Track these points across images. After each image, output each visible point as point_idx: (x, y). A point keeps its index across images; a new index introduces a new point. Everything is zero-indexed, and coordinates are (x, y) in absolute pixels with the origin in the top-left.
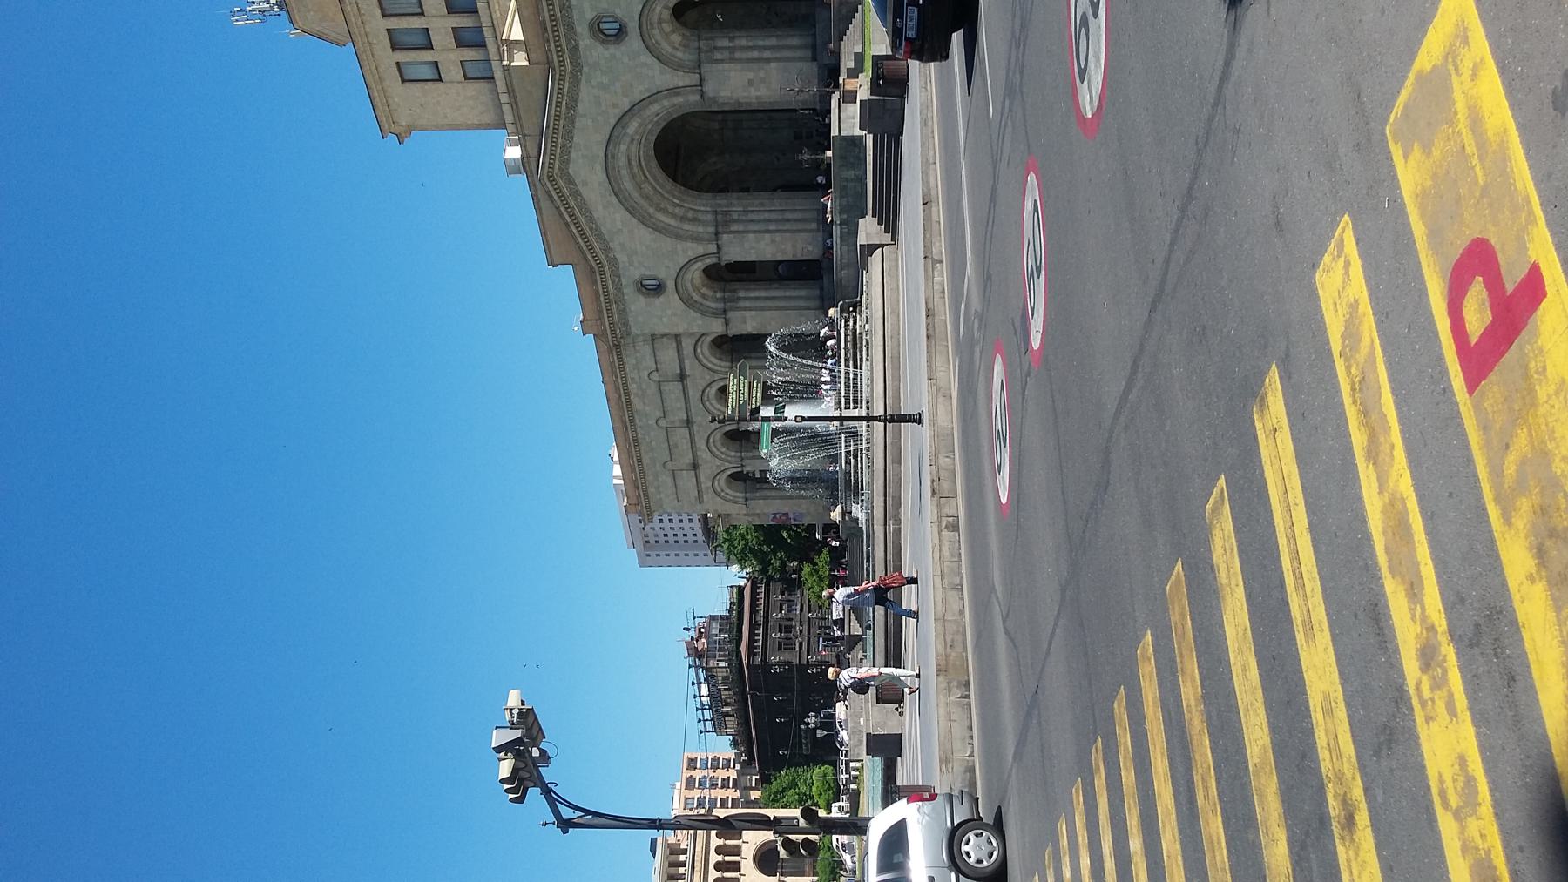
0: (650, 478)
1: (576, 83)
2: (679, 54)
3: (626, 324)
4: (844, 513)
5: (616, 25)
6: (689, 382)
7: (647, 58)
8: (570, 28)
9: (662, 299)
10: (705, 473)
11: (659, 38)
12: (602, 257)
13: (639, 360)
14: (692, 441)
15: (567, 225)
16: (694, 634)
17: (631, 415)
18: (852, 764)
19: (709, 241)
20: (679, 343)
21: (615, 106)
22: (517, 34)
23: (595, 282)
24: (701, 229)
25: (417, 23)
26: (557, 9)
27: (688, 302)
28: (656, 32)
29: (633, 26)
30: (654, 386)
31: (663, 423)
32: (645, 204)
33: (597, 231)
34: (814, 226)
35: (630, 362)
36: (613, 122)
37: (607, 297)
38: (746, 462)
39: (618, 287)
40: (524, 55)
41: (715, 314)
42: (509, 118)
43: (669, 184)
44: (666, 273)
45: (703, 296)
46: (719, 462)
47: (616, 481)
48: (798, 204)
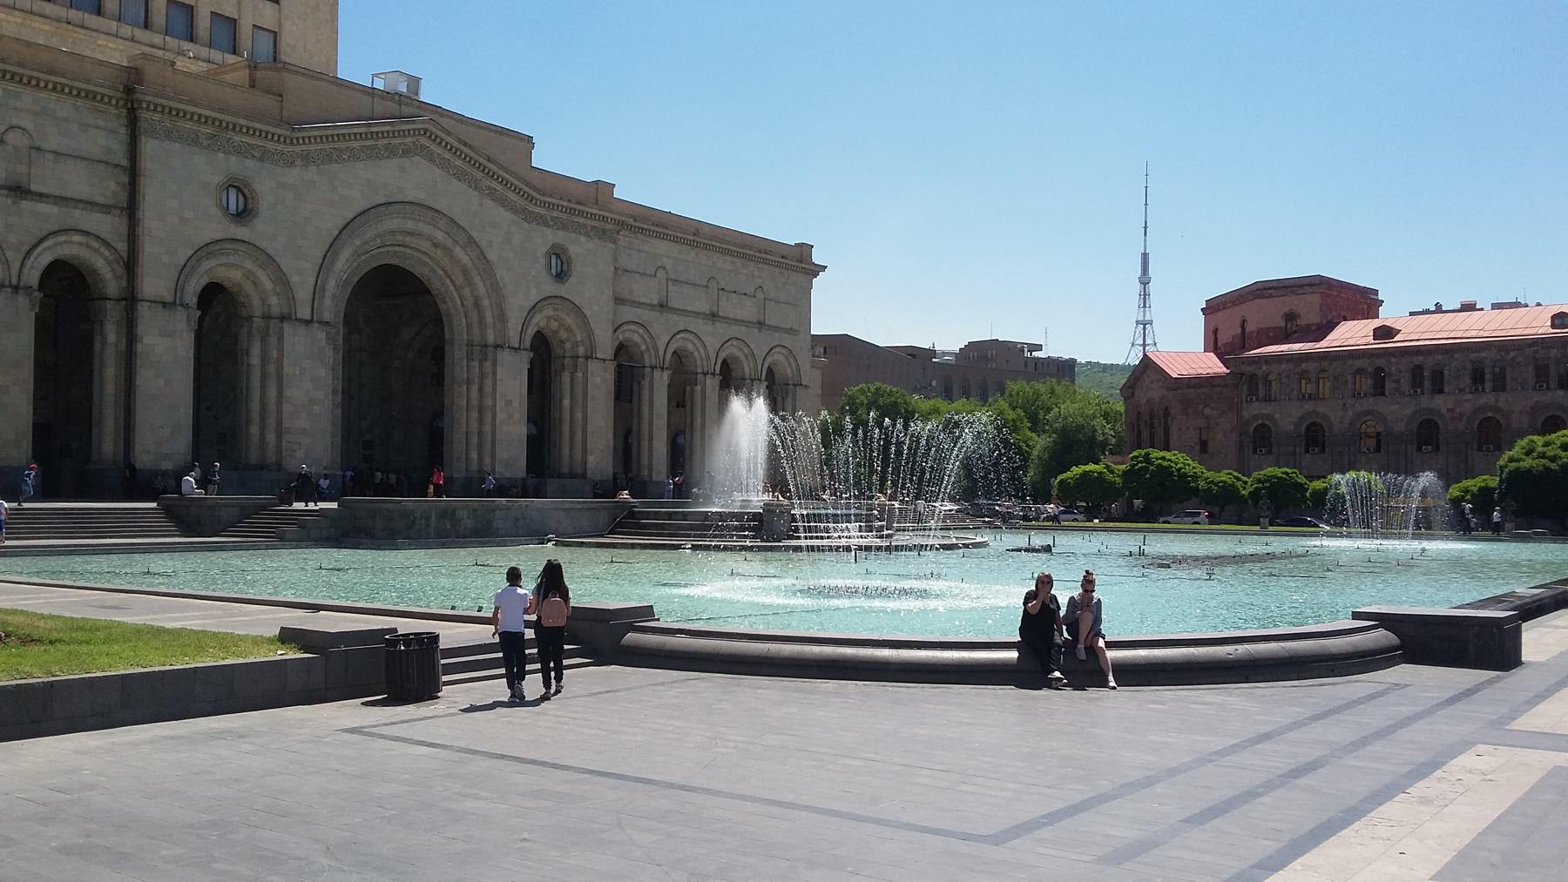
1: (514, 209)
3: (168, 135)
7: (534, 297)
8: (564, 226)
9: (215, 211)
12: (298, 149)
20: (105, 208)
26: (581, 220)
27: (206, 250)
28: (549, 311)
35: (64, 107)
36: (474, 234)
41: (178, 288)
44: (261, 230)
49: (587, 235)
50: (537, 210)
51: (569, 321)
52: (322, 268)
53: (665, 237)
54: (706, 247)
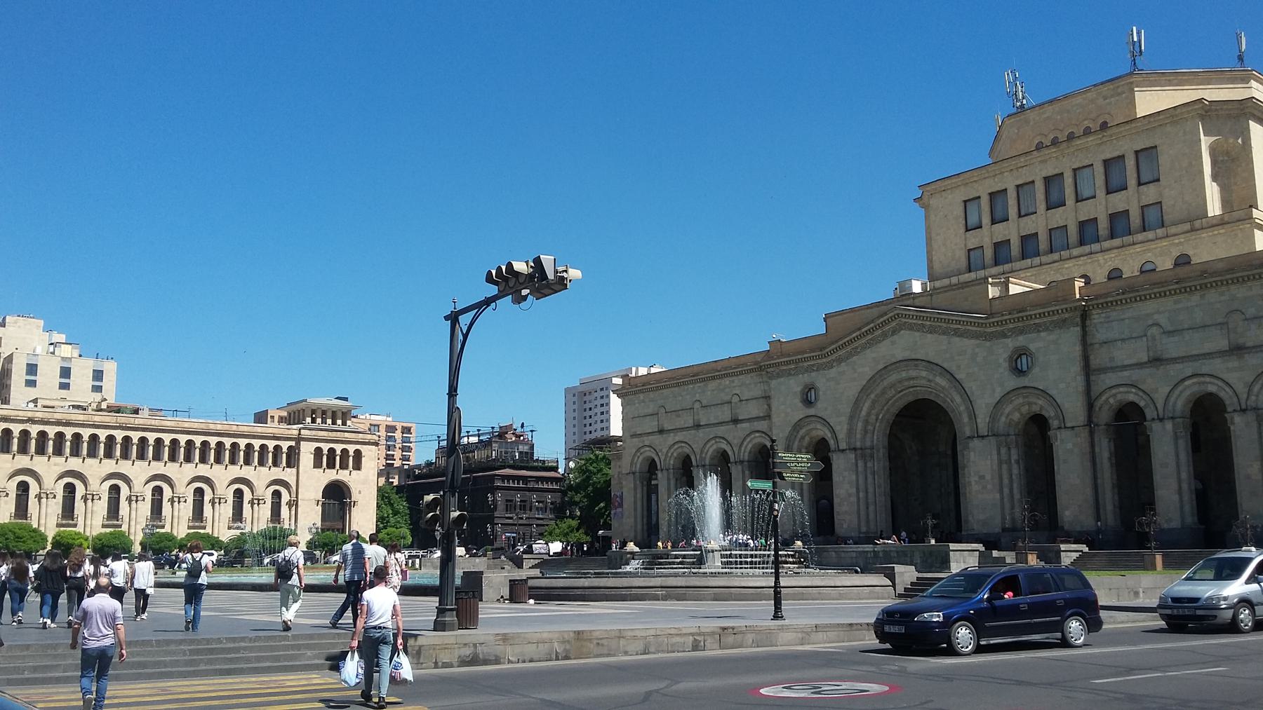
0: (652, 395)
1: (976, 336)
2: (1003, 419)
3: (779, 376)
4: (632, 553)
5: (1025, 368)
6: (731, 426)
8: (1021, 332)
9: (800, 404)
10: (656, 439)
11: (1016, 403)
12: (833, 357)
13: (749, 387)
14: (682, 429)
15: (860, 329)
16: (519, 430)
17: (703, 380)
19: (848, 443)
20: (763, 418)
21: (959, 367)
22: (1014, 289)
23: (812, 351)
24: (858, 436)
25: (1013, 212)
27: (797, 426)
28: (1021, 400)
29: (1024, 381)
30: (727, 398)
31: (697, 405)
32: (878, 391)
33: (855, 352)
34: (864, 529)
35: (747, 379)
36: (945, 365)
37: (801, 360)
38: (665, 473)
39: (809, 369)
40: (997, 295)
42: (938, 284)
43: (895, 410)
44: (821, 408)
45: (803, 438)
46: (665, 451)
47: (634, 369)
48: (881, 518)
49: (1047, 329)
50: (993, 329)
51: (1040, 402)
52: (852, 418)
53: (1144, 299)
54: (1204, 287)
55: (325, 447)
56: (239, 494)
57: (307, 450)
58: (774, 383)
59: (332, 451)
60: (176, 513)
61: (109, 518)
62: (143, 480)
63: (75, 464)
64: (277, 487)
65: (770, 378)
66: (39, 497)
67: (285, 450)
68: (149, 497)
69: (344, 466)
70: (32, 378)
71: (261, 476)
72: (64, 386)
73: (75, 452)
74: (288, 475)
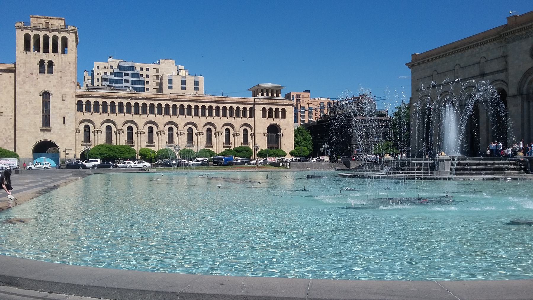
3: (514, 40)
13: (492, 51)
17: (462, 50)
18: (288, 164)
27: (526, 74)
31: (457, 67)
35: (490, 46)
41: (520, 89)
55: (267, 107)
56: (227, 131)
57: (258, 110)
58: (510, 46)
59: (271, 109)
60: (199, 140)
61: (226, 143)
62: (183, 125)
63: (152, 118)
64: (246, 127)
65: (508, 43)
66: (137, 133)
67: (248, 109)
68: (186, 133)
69: (277, 116)
70: (171, 85)
71: (237, 122)
72: (183, 88)
73: (152, 112)
74: (250, 121)
